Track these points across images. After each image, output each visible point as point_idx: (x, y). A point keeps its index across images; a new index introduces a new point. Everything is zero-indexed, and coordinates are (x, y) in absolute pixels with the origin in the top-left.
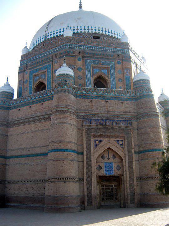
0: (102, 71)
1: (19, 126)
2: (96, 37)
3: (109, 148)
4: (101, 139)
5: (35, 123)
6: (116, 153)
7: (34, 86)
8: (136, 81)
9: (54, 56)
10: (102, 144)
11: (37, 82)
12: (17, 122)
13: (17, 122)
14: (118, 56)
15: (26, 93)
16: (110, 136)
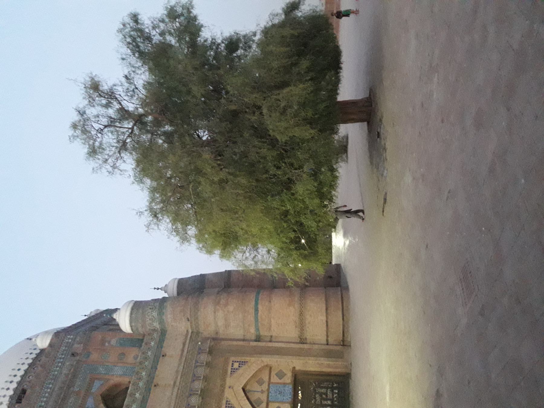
3: (244, 389)
8: (131, 326)
14: (73, 354)
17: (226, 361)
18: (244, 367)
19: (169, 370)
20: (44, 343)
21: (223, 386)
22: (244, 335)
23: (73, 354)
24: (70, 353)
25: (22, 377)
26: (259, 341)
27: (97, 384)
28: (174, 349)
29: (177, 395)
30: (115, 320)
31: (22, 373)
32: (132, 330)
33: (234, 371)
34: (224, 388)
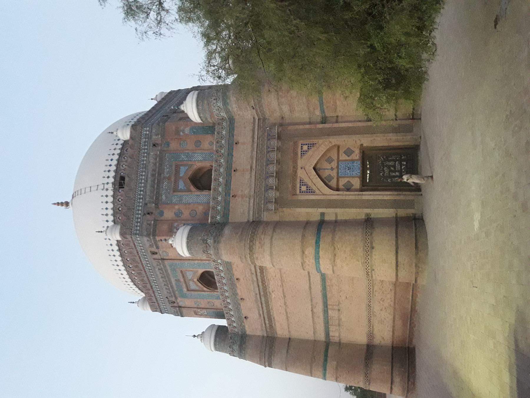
0: (181, 175)
1: (274, 318)
2: (120, 182)
3: (314, 168)
4: (298, 181)
5: (270, 293)
6: (323, 156)
7: (207, 293)
8: (200, 117)
9: (156, 256)
10: (306, 180)
11: (200, 285)
12: (267, 322)
13: (267, 322)
14: (154, 145)
15: (218, 304)
16: (294, 167)
17: (295, 143)
18: (313, 149)
19: (244, 155)
20: (125, 135)
21: (295, 168)
22: (310, 118)
23: (154, 145)
24: (152, 145)
25: (117, 165)
26: (325, 123)
27: (183, 170)
28: (245, 136)
29: (255, 178)
30: (183, 112)
31: (115, 162)
32: (202, 120)
33: (303, 153)
34: (297, 169)
